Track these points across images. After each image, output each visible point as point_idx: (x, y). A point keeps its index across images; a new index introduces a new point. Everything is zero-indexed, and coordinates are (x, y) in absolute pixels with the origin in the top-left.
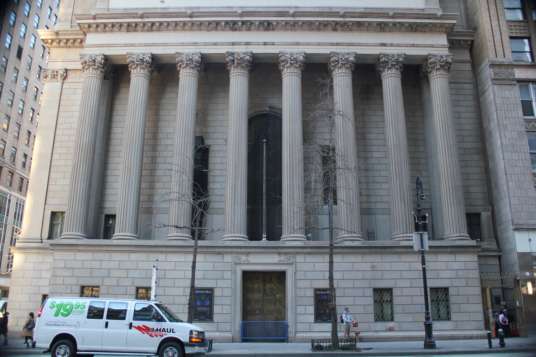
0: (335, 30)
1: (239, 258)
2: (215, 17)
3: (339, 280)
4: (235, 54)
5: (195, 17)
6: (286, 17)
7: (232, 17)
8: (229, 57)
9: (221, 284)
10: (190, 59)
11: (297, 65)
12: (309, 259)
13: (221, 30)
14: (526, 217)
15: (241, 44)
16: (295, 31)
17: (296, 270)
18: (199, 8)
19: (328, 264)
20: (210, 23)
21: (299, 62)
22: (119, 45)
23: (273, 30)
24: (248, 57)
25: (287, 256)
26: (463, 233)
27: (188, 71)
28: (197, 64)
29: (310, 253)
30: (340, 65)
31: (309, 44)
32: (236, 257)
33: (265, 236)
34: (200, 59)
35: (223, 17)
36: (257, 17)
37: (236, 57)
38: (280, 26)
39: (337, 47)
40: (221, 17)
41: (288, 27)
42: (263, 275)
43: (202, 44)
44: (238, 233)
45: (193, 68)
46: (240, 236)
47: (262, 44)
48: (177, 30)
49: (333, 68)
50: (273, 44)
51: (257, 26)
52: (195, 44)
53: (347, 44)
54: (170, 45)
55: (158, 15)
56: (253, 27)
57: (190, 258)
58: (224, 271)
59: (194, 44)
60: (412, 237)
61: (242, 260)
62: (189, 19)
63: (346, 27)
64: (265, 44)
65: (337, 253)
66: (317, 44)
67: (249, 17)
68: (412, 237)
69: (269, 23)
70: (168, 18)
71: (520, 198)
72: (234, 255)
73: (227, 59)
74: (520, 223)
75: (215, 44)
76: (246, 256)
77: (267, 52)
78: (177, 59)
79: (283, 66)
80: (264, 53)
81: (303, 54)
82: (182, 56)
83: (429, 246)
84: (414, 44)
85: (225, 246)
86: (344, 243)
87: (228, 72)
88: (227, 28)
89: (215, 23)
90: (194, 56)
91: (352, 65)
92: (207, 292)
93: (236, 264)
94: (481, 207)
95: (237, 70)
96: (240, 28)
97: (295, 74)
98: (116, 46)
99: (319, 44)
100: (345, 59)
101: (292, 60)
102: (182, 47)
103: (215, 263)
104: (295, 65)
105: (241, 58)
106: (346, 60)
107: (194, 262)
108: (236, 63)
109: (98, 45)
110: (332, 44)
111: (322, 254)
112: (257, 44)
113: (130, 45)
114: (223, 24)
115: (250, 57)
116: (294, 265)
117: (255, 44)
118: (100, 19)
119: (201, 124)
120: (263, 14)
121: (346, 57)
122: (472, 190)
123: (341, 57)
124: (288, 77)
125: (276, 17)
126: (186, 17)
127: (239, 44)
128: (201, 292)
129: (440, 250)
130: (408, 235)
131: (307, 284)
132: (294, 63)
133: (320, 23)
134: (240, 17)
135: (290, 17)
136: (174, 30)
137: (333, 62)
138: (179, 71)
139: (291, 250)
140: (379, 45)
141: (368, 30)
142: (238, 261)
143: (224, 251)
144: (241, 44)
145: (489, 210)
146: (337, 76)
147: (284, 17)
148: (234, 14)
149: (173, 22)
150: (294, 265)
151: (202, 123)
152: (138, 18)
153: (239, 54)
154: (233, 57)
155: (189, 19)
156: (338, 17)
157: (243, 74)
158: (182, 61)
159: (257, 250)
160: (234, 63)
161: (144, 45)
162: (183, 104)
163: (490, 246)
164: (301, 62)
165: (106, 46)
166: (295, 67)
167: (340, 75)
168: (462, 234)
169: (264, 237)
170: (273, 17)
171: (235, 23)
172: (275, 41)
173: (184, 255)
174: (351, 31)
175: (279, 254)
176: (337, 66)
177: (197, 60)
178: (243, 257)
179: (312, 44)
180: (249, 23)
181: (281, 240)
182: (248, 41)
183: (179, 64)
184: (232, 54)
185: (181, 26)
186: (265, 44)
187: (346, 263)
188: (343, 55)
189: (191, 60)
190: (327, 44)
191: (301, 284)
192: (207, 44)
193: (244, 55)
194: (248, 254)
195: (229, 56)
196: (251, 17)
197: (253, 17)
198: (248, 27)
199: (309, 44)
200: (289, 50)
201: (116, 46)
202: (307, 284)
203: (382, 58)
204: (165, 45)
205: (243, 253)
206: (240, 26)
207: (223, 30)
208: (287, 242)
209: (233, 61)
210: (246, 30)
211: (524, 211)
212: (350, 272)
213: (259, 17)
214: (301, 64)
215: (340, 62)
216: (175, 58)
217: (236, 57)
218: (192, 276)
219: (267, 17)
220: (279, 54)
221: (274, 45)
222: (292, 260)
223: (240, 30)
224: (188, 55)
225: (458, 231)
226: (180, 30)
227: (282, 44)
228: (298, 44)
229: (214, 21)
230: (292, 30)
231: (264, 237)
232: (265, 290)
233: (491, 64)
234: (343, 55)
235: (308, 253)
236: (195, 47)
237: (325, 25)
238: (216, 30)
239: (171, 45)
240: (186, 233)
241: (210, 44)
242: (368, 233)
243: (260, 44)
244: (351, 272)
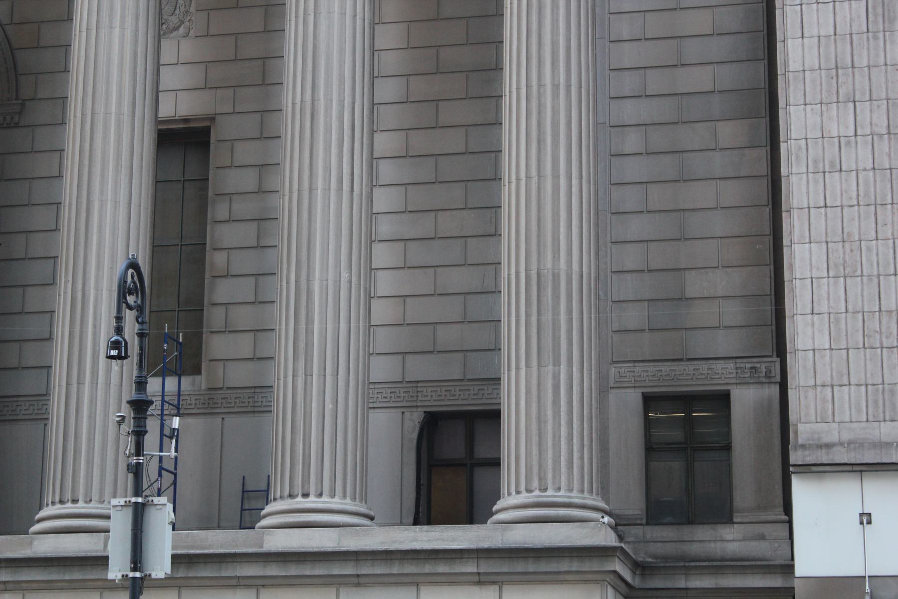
14: (859, 411)
26: (306, 495)
60: (108, 517)
68: (108, 517)
71: (837, 321)
74: (826, 439)
83: (174, 557)
86: (35, 543)
94: (730, 366)
122: (695, 285)
129: (428, 568)
130: (93, 508)
145: (768, 375)
163: (753, 544)
168: (549, 493)
211: (853, 381)
225: (535, 483)
242: (243, 492)
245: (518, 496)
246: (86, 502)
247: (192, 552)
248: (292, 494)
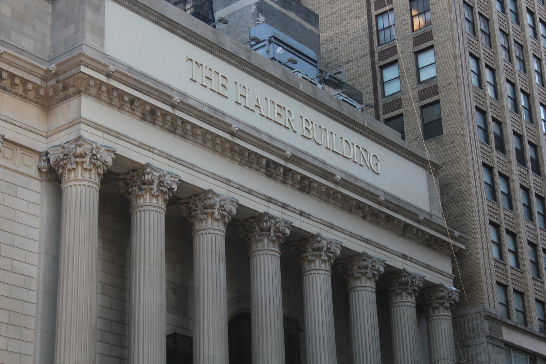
5: (237, 137)
13: (256, 169)
15: (278, 203)
16: (328, 204)
18: (223, 114)
22: (133, 142)
50: (309, 217)
53: (375, 244)
55: (196, 112)
59: (227, 182)
64: (302, 213)
77: (304, 228)
84: (429, 265)
98: (129, 140)
109: (103, 127)
112: (293, 210)
113: (148, 148)
118: (116, 80)
120: (309, 166)
126: (227, 132)
134: (334, 183)
140: (401, 255)
141: (391, 230)
148: (280, 152)
152: (168, 105)
161: (165, 155)
165: (114, 134)
172: (312, 214)
179: (345, 232)
182: (286, 201)
186: (302, 213)
192: (241, 188)
200: (327, 234)
201: (129, 140)
203: (405, 277)
204: (192, 167)
210: (281, 181)
219: (311, 172)
221: (309, 218)
226: (210, 148)
228: (331, 226)
230: (325, 201)
233: (488, 316)
236: (226, 186)
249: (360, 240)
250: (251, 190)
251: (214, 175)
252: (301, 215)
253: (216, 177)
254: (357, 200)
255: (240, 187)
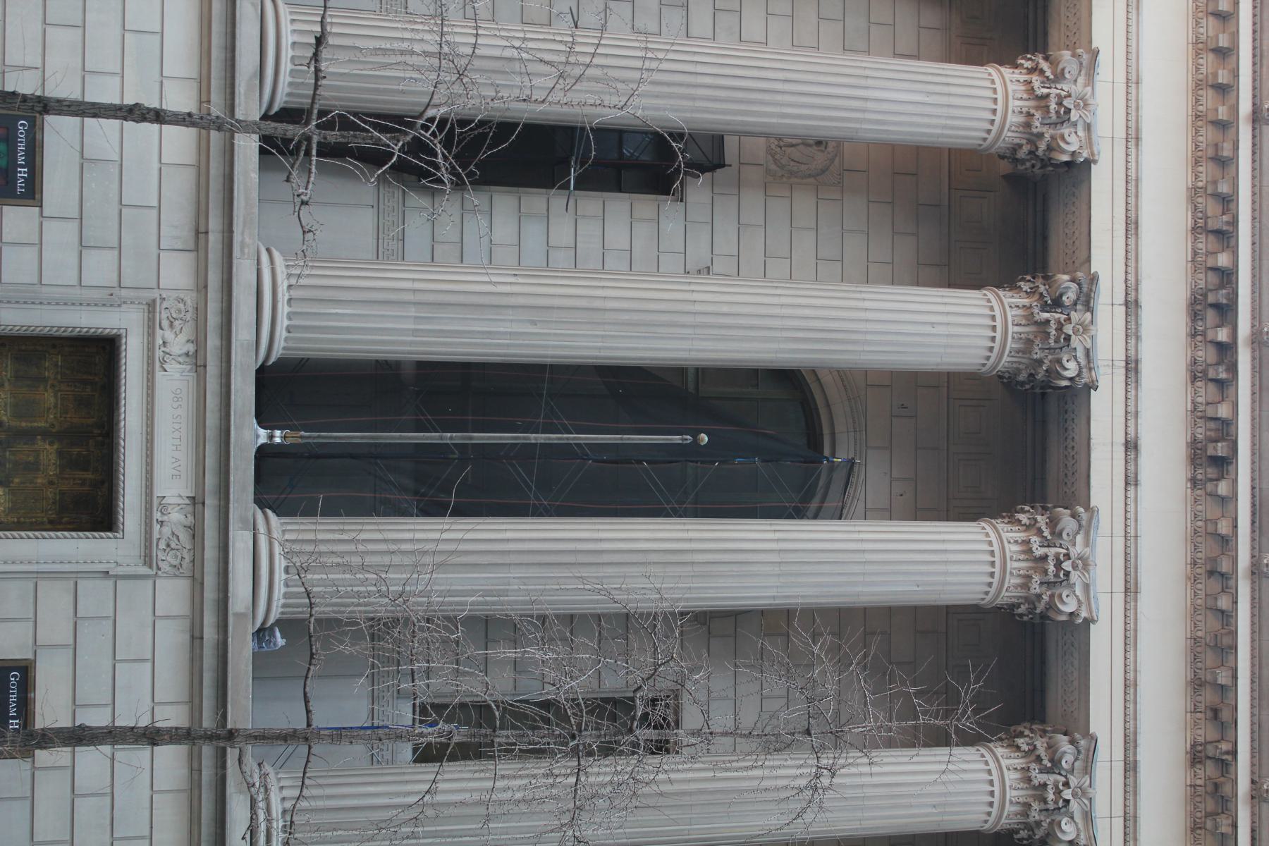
0: (1196, 756)
1: (177, 323)
2: (1253, 227)
3: (69, 772)
4: (1088, 315)
5: (1254, 137)
6: (1253, 540)
7: (1253, 301)
8: (1074, 286)
9: (60, 236)
10: (1068, 111)
11: (1036, 588)
12: (172, 639)
13: (1195, 253)
15: (1133, 341)
17: (117, 577)
19: (144, 722)
20: (1227, 202)
21: (1052, 596)
23: (1194, 482)
24: (1071, 369)
25: (184, 537)
27: (1014, 104)
28: (1042, 146)
29: (197, 642)
30: (1040, 778)
31: (1130, 640)
32: (181, 306)
33: (278, 440)
34: (1065, 158)
35: (1253, 260)
36: (1253, 410)
37: (1075, 316)
38: (1213, 511)
39: (1119, 767)
40: (1254, 251)
41: (1208, 549)
42: (96, 431)
43: (1133, 165)
44: (289, 318)
45: (1028, 125)
46: (278, 328)
47: (1131, 430)
48: (1197, 54)
49: (1025, 747)
50: (1131, 481)
51: (1210, 413)
52: (1133, 137)
53: (1131, 810)
54: (1133, 22)
56: (1207, 392)
57: (180, 99)
58: (116, 252)
59: (1132, 132)
61: (169, 335)
62: (1245, 107)
63: (1210, 805)
64: (1131, 446)
65: (196, 766)
66: (1131, 676)
67: (1253, 377)
69: (1224, 464)
70: (1254, 15)
72: (190, 299)
73: (1066, 277)
75: (1132, 226)
76: (187, 354)
78: (1066, 54)
79: (1032, 526)
80: (1092, 442)
81: (1084, 614)
82: (1081, 80)
85: (235, 261)
86: (242, 797)
87: (1005, 280)
88: (1202, 276)
89: (1228, 223)
90: (1081, 133)
91: (1039, 834)
92: (22, 173)
93: (151, 305)
95: (1017, 320)
96: (1204, 334)
97: (997, 575)
99: (1130, 686)
100: (1067, 802)
101: (1058, 564)
102: (1121, 77)
103: (155, 212)
104: (1037, 578)
105: (1068, 338)
106: (1061, 803)
107: (158, 116)
108: (1046, 315)
110: (1130, 742)
111: (191, 696)
112: (1131, 409)
114: (1223, 260)
115: (1071, 379)
116: (144, 570)
117: (1131, 403)
119: (775, 161)
121: (1074, 806)
123: (1073, 781)
124: (986, 547)
125: (1253, 496)
126: (1254, 97)
127: (1132, 332)
128: (21, 147)
131: (55, 628)
132: (1046, 572)
133: (1227, 691)
134: (1253, 334)
135: (1253, 557)
136: (1197, 41)
137: (1051, 747)
138: (1016, 66)
139: (210, 553)
142: (162, 316)
143: (211, 256)
144: (1133, 341)
146: (987, 763)
147: (1253, 531)
149: (1235, 36)
150: (144, 570)
151: (782, 167)
153: (1085, 328)
154: (1075, 304)
155: (1245, 107)
156: (1253, 773)
157: (997, 346)
158: (1060, 77)
159: (212, 402)
160: (1045, 308)
162: (870, 82)
164: (1051, 606)
166: (1029, 577)
167: (995, 777)
169: (271, 437)
170: (1253, 480)
171: (1226, 312)
173: (195, 75)
174: (1193, 830)
175: (196, 502)
176: (1033, 766)
177: (1062, 144)
178: (182, 338)
179: (1131, 655)
180: (1223, 376)
181: (259, 512)
182: (1146, 368)
183: (1044, 65)
184: (1086, 301)
185: (1215, 75)
186: (1131, 446)
187: (148, 805)
188: (1084, 793)
189: (1064, 118)
190: (1130, 718)
191: (55, 599)
192: (1132, 187)
193: (1080, 354)
194: (197, 362)
195: (1079, 285)
196: (1253, 385)
197: (1253, 393)
198: (1205, 372)
199: (1130, 640)
202: (55, 628)
205: (199, 341)
206: (1210, 336)
207: (1193, 261)
208: (248, 535)
209: (1057, 303)
210: (1194, 362)
212: (108, 822)
213: (1253, 419)
214: (1043, 603)
215: (1050, 779)
216: (1072, 47)
217: (1075, 316)
218: (94, 104)
220: (1087, 507)
221: (1127, 483)
222: (167, 560)
223: (1193, 334)
224: (1086, 105)
226: (1197, 69)
227: (1131, 523)
228: (1131, 590)
229: (1234, 222)
231: (271, 437)
232: (28, 435)
234: (1082, 793)
235: (197, 634)
237: (1215, 712)
238: (1194, 229)
239: (1133, 29)
240: (290, 84)
241: (1132, 200)
243: (1131, 423)
244: (109, 828)
245: (279, 799)
246: (288, 313)
247: (230, 640)
248: (292, 301)
249: (1125, 736)
250: (1137, 228)
251: (1137, 83)
252: (1127, 443)
253: (1134, 92)
254: (1236, 678)
255: (1133, 183)
